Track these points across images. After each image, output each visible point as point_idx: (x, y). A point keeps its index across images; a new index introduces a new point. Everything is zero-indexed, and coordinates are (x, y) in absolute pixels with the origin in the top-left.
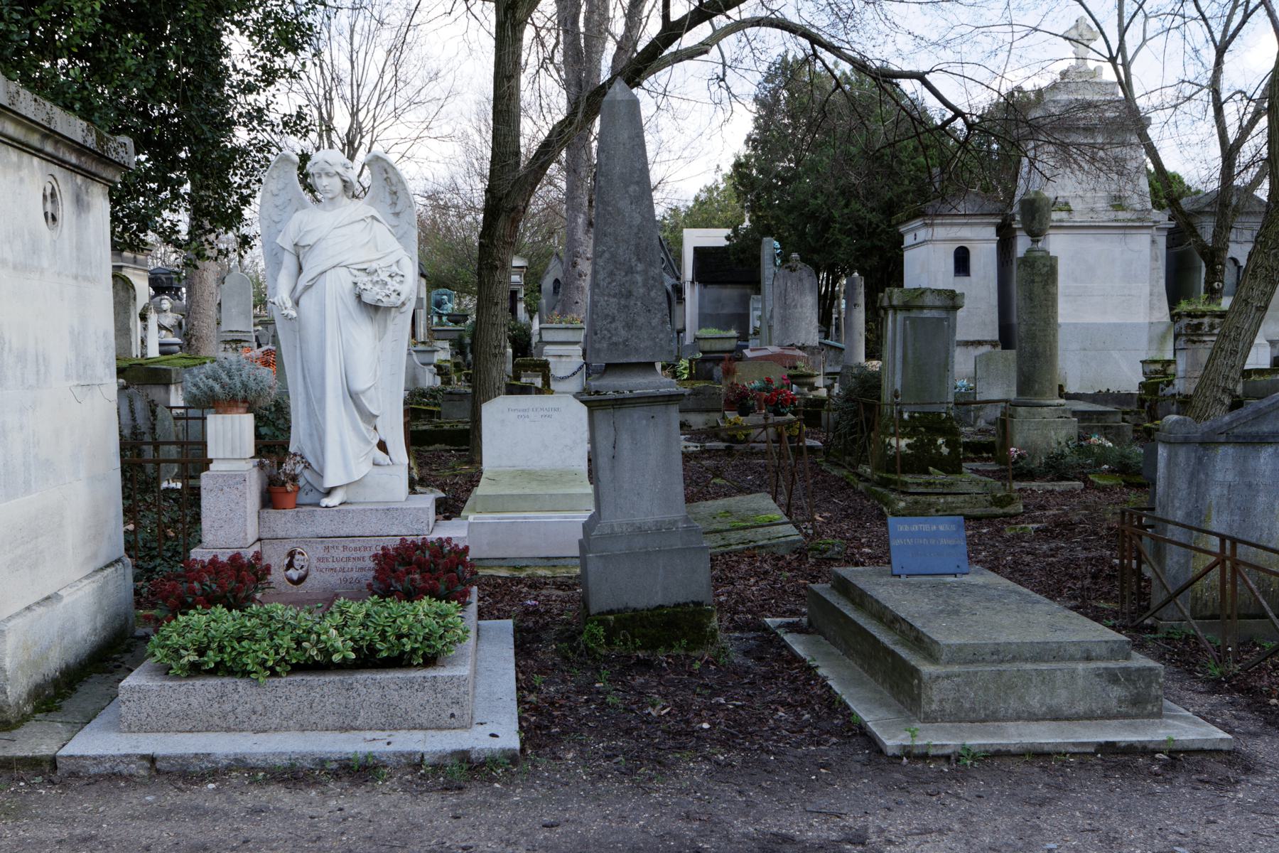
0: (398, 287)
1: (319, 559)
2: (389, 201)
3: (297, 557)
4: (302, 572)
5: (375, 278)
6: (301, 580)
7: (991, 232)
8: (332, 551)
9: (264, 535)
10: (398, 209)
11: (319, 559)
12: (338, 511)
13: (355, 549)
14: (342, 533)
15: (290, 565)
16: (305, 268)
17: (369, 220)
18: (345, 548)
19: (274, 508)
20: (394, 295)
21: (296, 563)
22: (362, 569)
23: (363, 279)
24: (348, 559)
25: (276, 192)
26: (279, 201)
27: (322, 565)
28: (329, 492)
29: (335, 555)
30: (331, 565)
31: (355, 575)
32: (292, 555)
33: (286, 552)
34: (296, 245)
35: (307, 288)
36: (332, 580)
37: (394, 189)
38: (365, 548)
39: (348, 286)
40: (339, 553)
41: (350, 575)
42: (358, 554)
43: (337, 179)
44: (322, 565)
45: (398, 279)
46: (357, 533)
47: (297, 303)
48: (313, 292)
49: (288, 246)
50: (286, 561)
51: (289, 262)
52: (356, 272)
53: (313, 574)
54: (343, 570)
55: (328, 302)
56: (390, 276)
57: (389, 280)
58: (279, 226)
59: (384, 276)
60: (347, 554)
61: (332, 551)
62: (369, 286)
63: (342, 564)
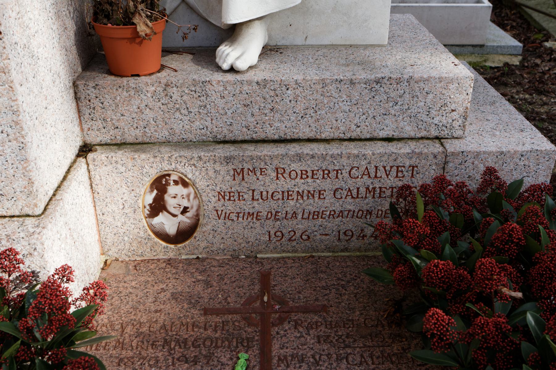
1: (221, 195)
3: (173, 189)
4: (186, 220)
6: (183, 235)
8: (250, 178)
9: (93, 138)
11: (221, 195)
12: (262, 84)
13: (304, 174)
14: (271, 133)
15: (158, 207)
18: (279, 172)
19: (114, 71)
21: (170, 202)
22: (316, 215)
24: (287, 195)
27: (230, 207)
28: (232, 32)
29: (259, 186)
30: (247, 206)
31: (301, 226)
32: (160, 185)
33: (148, 181)
36: (251, 236)
38: (326, 174)
40: (269, 183)
41: (291, 224)
42: (311, 185)
44: (230, 207)
46: (305, 132)
50: (150, 198)
53: (208, 225)
54: (274, 216)
60: (285, 184)
61: (250, 178)
63: (273, 205)
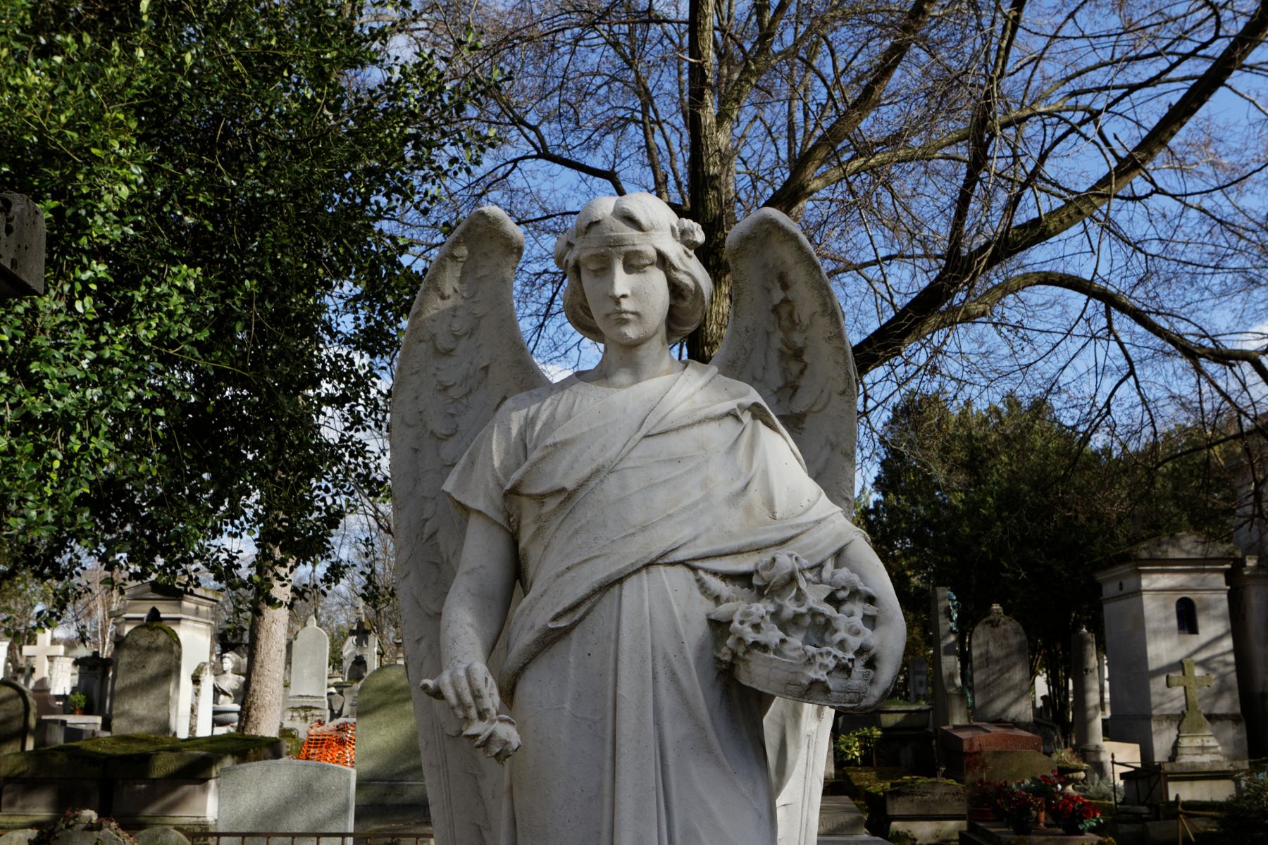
0: (869, 637)
2: (776, 380)
5: (790, 607)
7: (1219, 580)
10: (799, 405)
16: (543, 571)
17: (746, 418)
20: (858, 668)
23: (746, 611)
25: (444, 342)
26: (452, 371)
34: (513, 493)
35: (551, 639)
37: (798, 339)
39: (696, 631)
43: (657, 278)
45: (859, 608)
47: (508, 693)
48: (571, 652)
49: (480, 498)
51: (479, 553)
52: (716, 584)
55: (626, 689)
56: (832, 599)
57: (828, 610)
58: (447, 449)
59: (815, 597)
62: (772, 635)
